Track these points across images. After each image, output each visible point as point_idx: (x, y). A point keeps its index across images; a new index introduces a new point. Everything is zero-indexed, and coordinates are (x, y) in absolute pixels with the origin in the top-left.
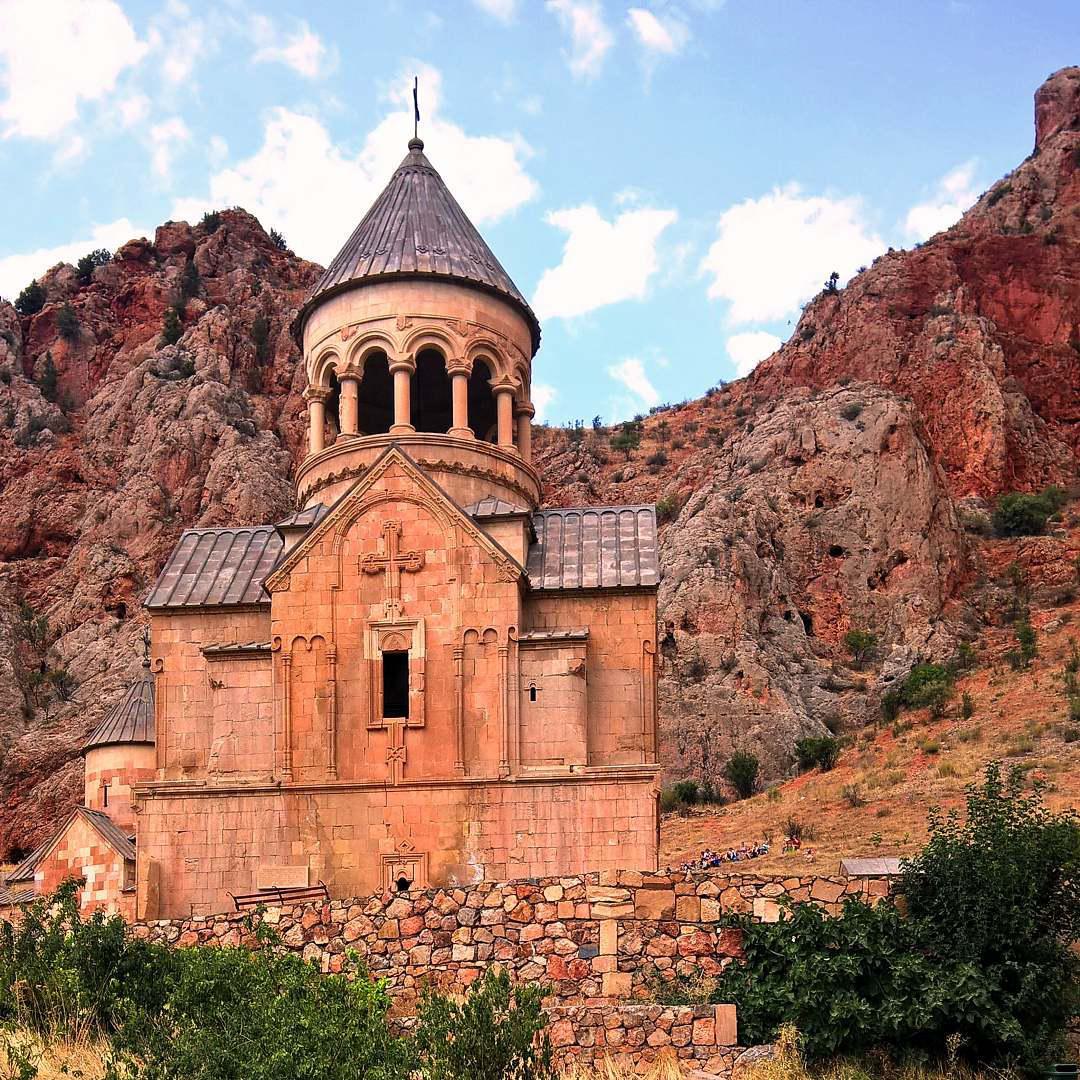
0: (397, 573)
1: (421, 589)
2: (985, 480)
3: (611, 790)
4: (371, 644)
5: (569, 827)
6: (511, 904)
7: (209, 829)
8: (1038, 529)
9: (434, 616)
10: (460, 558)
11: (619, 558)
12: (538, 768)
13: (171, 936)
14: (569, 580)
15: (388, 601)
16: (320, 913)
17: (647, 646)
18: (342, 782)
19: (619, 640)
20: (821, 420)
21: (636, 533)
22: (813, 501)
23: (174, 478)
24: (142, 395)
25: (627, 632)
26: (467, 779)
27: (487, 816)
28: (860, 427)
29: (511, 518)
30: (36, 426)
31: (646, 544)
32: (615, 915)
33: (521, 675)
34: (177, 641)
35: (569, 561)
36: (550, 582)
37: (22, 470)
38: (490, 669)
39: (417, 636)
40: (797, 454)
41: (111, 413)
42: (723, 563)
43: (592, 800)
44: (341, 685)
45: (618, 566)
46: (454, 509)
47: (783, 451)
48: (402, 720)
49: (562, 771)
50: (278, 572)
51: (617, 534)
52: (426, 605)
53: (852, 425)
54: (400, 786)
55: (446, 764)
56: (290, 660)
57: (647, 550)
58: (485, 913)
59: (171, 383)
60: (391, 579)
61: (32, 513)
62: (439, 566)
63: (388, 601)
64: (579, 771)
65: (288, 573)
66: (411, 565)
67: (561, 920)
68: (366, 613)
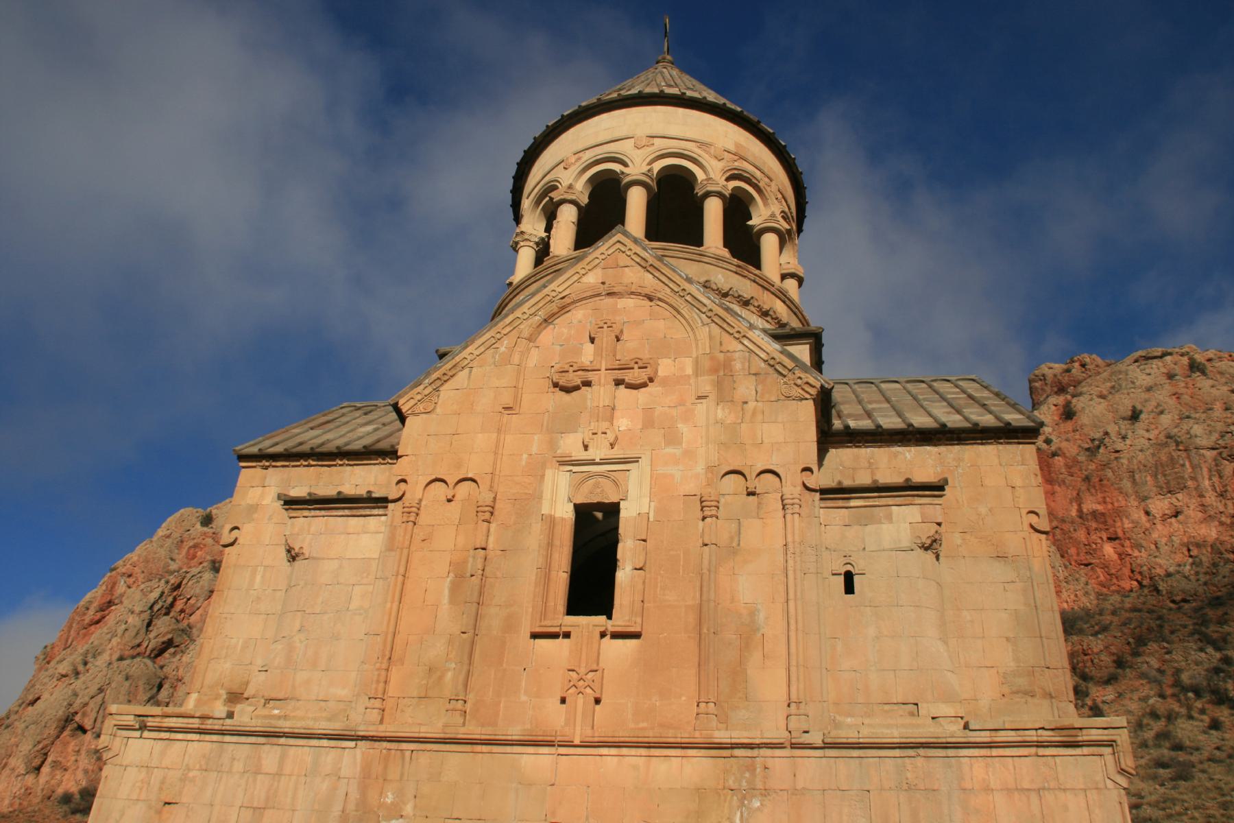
1: (648, 411)
9: (670, 450)
26: (722, 736)
43: (988, 789)
48: (602, 619)
49: (924, 730)
50: (422, 387)
56: (413, 515)
64: (953, 731)
65: (437, 390)
68: (552, 445)
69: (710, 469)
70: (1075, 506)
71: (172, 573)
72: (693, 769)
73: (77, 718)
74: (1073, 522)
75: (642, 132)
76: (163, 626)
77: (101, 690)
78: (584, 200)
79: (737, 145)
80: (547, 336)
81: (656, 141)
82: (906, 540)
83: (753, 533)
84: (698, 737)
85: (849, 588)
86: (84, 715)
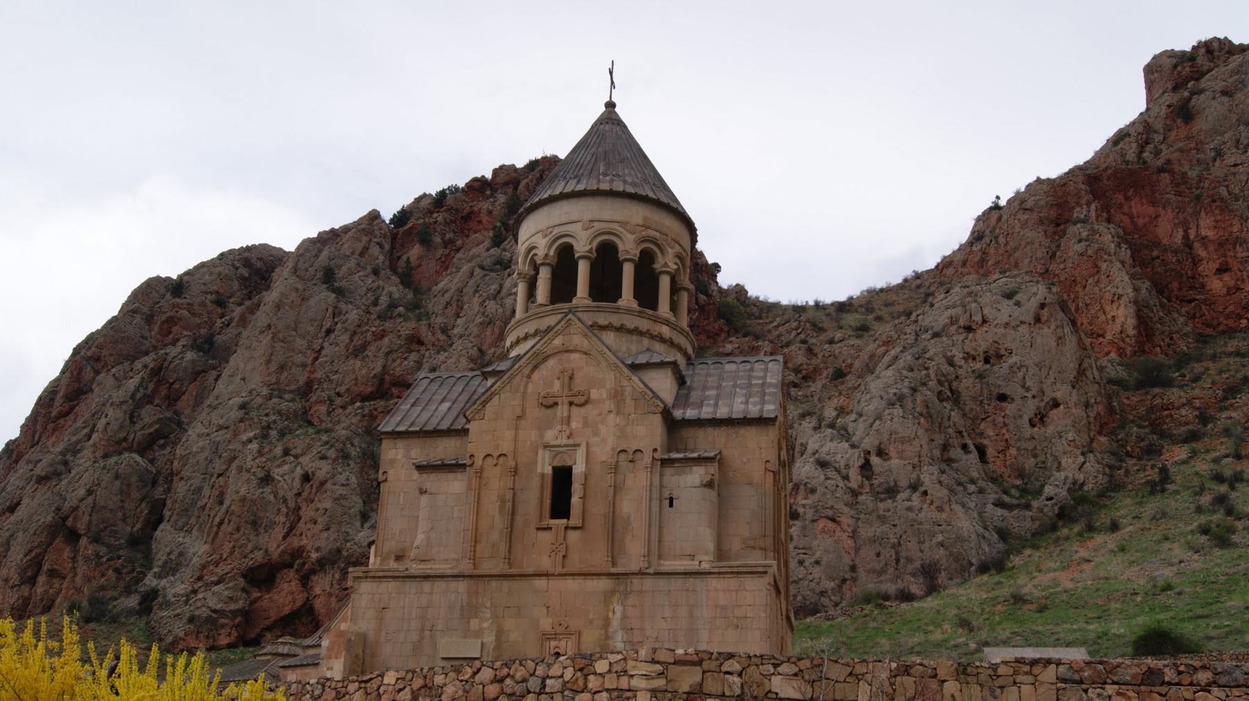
0: (566, 407)
2: (1122, 345)
3: (732, 582)
4: (543, 460)
6: (568, 674)
8: (1168, 384)
10: (617, 395)
11: (748, 397)
13: (317, 693)
14: (706, 412)
15: (559, 427)
16: (425, 677)
17: (768, 465)
18: (514, 571)
19: (745, 460)
20: (986, 299)
21: (765, 377)
22: (982, 358)
23: (489, 341)
24: (471, 283)
25: (752, 454)
26: (613, 570)
27: (630, 602)
28: (1018, 304)
29: (661, 365)
30: (393, 305)
31: (771, 385)
32: (650, 687)
33: (661, 486)
34: (400, 456)
35: (708, 398)
36: (690, 413)
37: (380, 336)
38: (638, 481)
39: (580, 455)
40: (967, 324)
41: (447, 296)
43: (716, 590)
44: (518, 494)
45: (747, 402)
47: (957, 321)
48: (565, 521)
49: (692, 565)
51: (750, 377)
53: (1011, 302)
54: (560, 575)
55: (598, 558)
57: (772, 390)
58: (548, 682)
59: (493, 274)
60: (562, 410)
61: (384, 367)
63: (559, 427)
64: (706, 566)
66: (581, 399)
67: (607, 690)
68: (541, 436)
69: (613, 449)
70: (1181, 233)
71: (147, 353)
72: (603, 584)
73: (69, 523)
74: (1176, 252)
75: (587, 217)
76: (149, 414)
77: (90, 492)
78: (554, 261)
79: (645, 219)
80: (536, 376)
81: (596, 224)
82: (697, 481)
83: (630, 481)
84: (604, 571)
85: (671, 505)
86: (75, 519)
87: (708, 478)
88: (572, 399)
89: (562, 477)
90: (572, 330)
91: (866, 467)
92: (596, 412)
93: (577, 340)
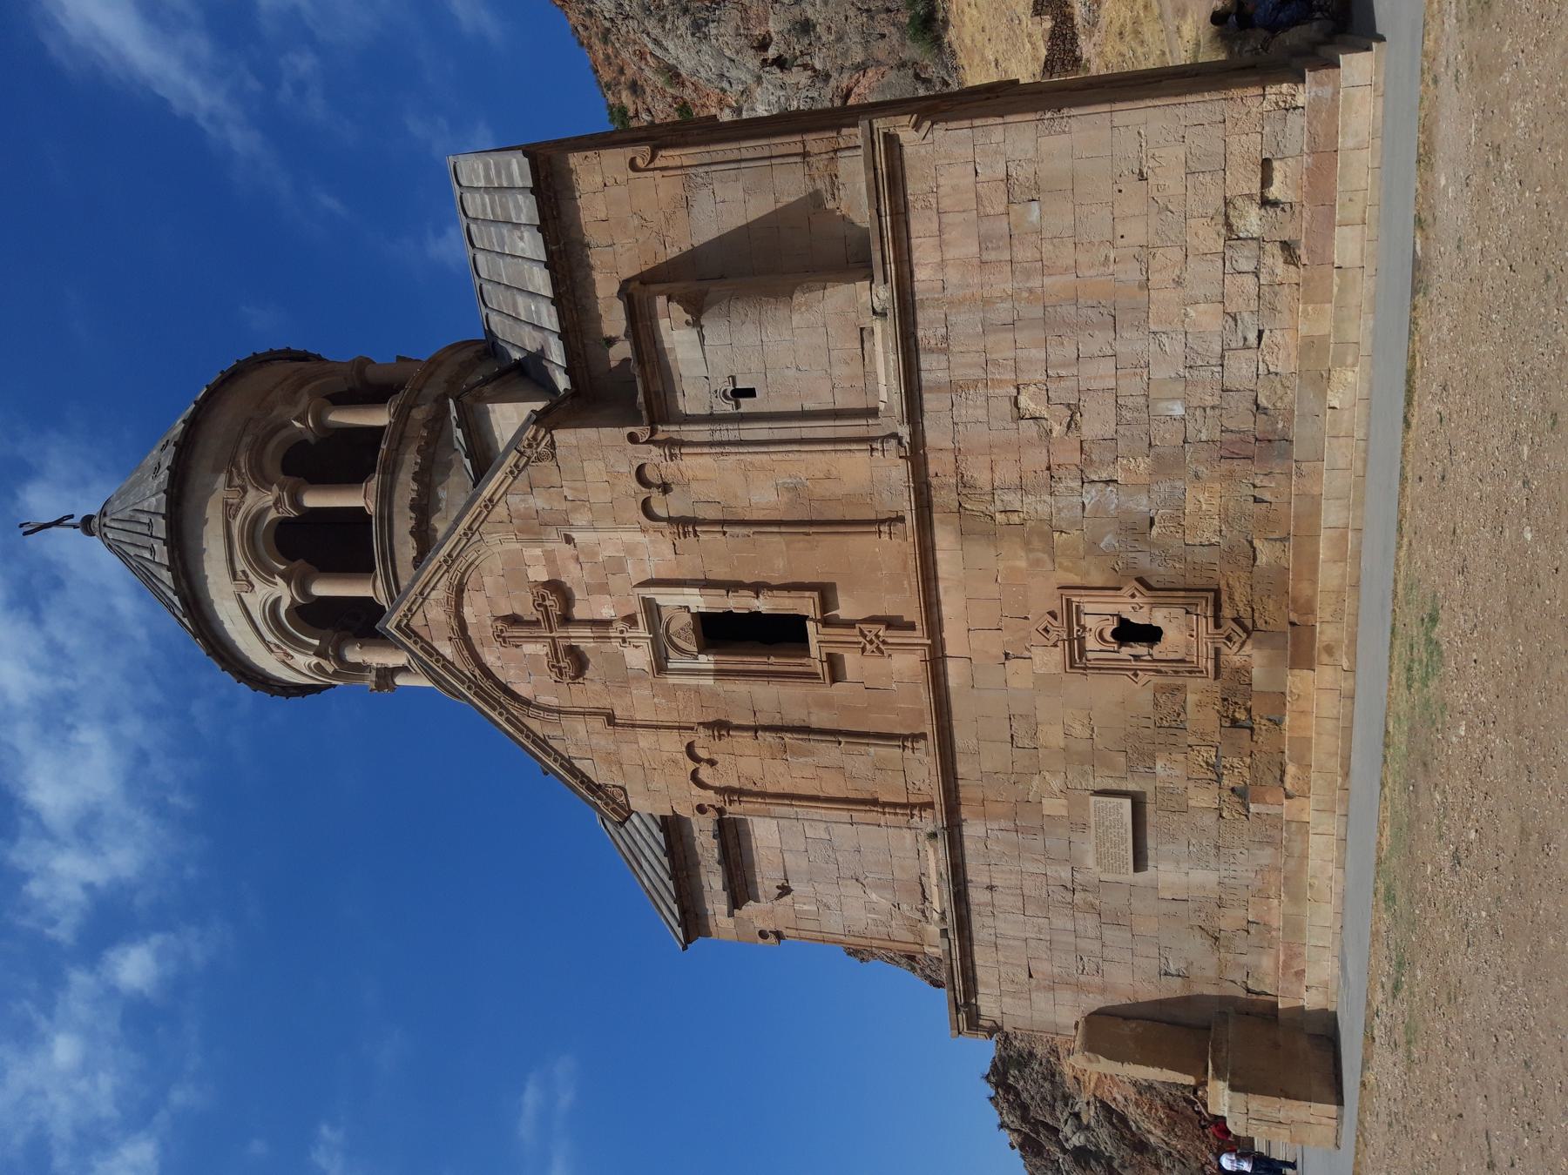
0: (573, 631)
1: (590, 590)
3: (921, 226)
5: (1003, 312)
7: (1023, 935)
10: (533, 527)
12: (882, 380)
15: (616, 643)
17: (639, 162)
18: (929, 728)
26: (911, 519)
27: (982, 478)
33: (711, 418)
42: (704, 14)
43: (942, 264)
46: (455, 537)
48: (810, 626)
52: (616, 582)
55: (891, 552)
60: (582, 638)
62: (550, 559)
63: (616, 643)
64: (883, 294)
65: (599, 786)
68: (640, 676)
72: (945, 540)
80: (523, 689)
82: (691, 335)
85: (750, 393)
87: (677, 310)
88: (554, 621)
89: (718, 632)
90: (417, 622)
91: (781, 63)
92: (574, 568)
93: (435, 612)
